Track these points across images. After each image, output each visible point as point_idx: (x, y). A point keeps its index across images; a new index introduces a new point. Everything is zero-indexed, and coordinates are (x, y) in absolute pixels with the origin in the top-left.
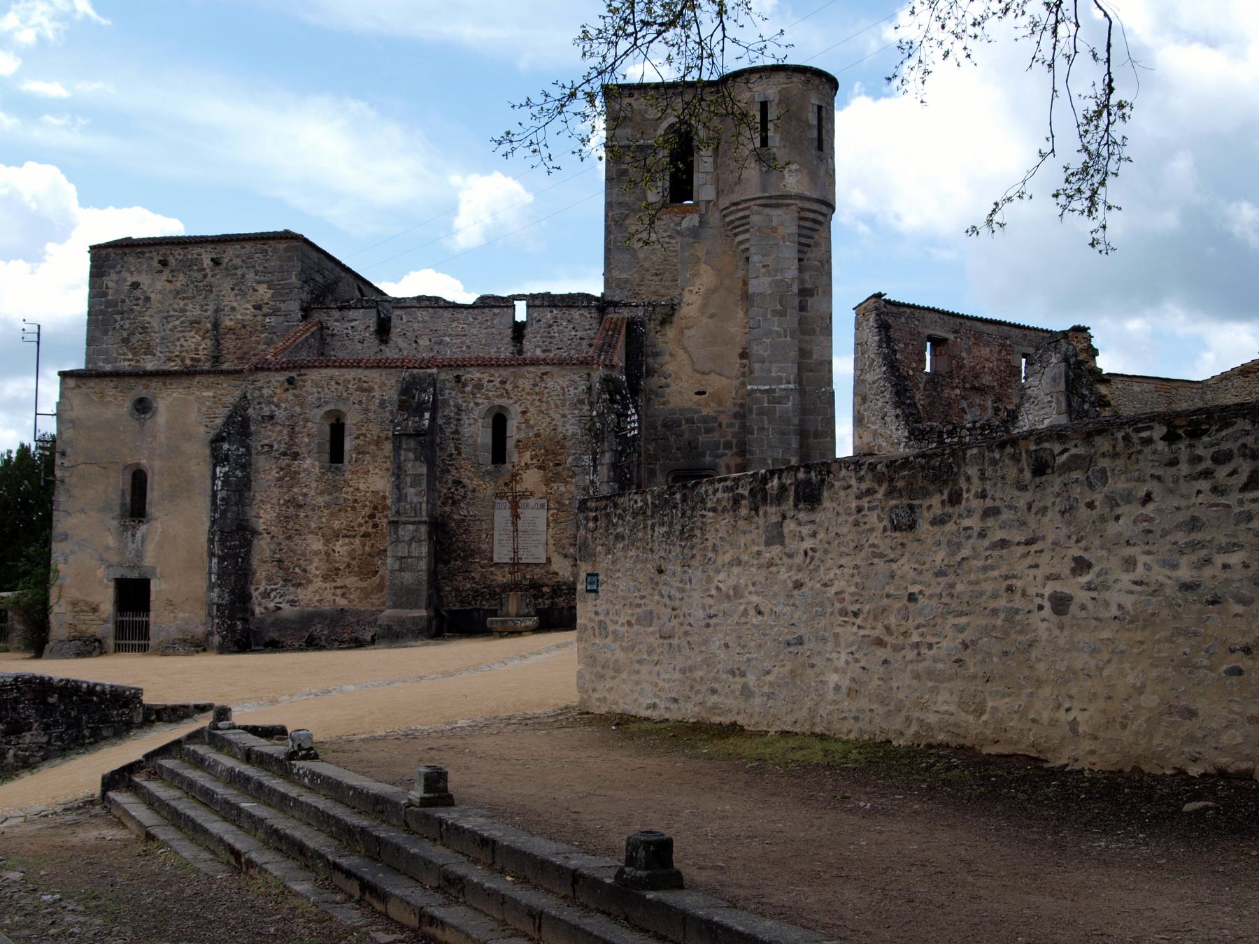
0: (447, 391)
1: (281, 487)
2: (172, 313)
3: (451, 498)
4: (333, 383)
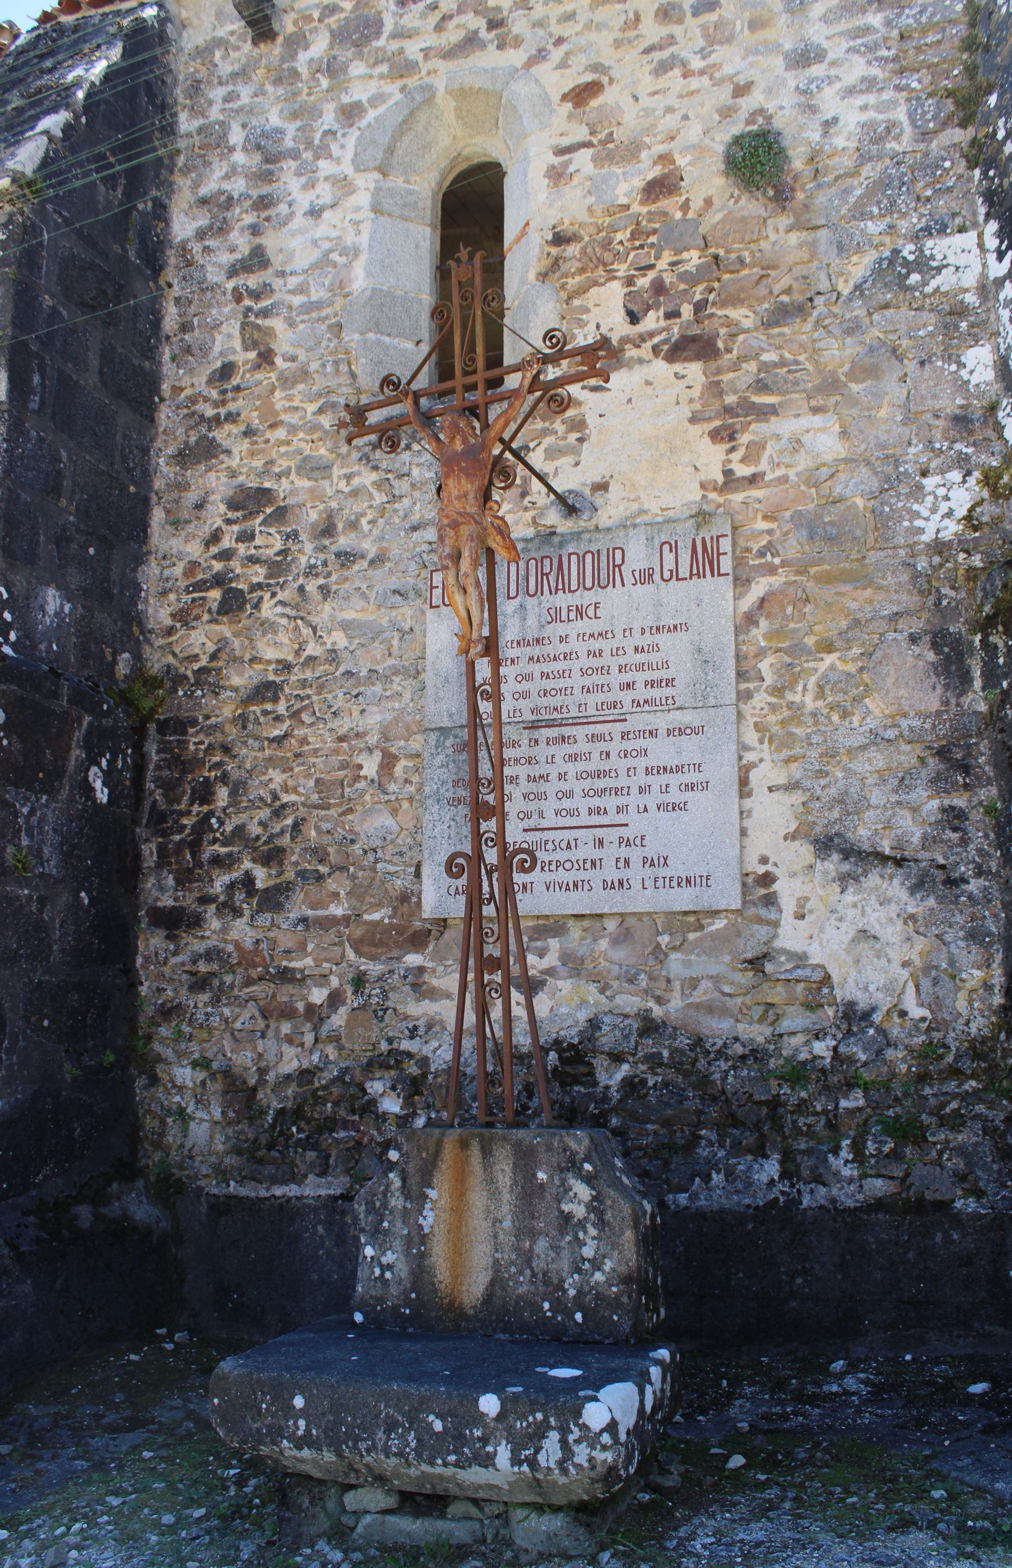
0: (218, 93)
3: (219, 580)
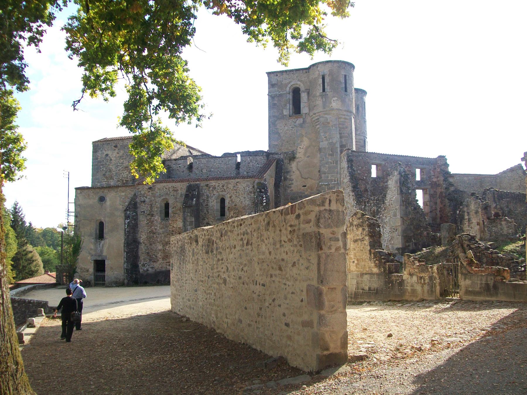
0: (203, 190)
1: (148, 226)
2: (119, 164)
4: (165, 188)
